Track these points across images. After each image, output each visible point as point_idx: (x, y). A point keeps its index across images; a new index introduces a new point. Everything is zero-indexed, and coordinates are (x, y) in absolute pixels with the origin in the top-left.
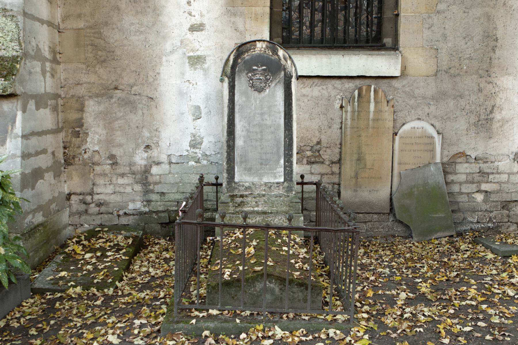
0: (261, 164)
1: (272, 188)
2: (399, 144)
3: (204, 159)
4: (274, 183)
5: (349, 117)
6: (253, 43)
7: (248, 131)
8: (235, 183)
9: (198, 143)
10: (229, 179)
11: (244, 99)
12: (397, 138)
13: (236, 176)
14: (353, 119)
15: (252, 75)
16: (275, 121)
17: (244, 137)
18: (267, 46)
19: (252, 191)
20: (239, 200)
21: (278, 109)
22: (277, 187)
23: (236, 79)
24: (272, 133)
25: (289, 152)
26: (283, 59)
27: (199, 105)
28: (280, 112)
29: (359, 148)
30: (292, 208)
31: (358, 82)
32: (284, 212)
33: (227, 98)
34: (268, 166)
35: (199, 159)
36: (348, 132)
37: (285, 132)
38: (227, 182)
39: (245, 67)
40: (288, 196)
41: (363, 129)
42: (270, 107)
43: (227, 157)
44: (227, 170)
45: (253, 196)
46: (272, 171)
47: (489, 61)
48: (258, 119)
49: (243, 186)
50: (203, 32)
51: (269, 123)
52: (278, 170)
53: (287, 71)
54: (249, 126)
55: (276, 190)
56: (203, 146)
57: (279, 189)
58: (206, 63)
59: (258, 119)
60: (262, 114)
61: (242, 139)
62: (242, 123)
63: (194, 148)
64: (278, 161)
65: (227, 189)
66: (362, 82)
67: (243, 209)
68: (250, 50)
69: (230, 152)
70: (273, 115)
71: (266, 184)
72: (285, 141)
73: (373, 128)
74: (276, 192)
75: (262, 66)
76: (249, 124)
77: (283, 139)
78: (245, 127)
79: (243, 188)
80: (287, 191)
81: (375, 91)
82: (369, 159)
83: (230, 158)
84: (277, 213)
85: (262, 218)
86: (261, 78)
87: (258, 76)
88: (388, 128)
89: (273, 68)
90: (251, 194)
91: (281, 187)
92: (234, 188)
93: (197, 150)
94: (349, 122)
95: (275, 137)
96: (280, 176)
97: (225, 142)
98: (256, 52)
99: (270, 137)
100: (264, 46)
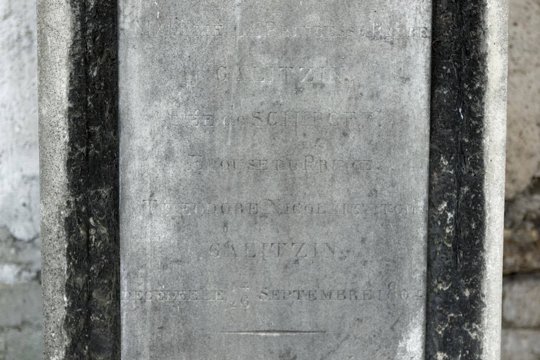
16: (374, 95)
17: (176, 192)
21: (393, 18)
24: (355, 167)
25: (456, 289)
28: (404, 41)
43: (67, 323)
48: (265, 80)
51: (332, 104)
54: (212, 128)
60: (292, 51)
61: (167, 205)
62: (163, 107)
69: (89, 287)
70: (362, 57)
72: (432, 221)
77: (421, 204)
78: (181, 131)
95: (373, 193)
97: (57, 229)
99: (339, 198)
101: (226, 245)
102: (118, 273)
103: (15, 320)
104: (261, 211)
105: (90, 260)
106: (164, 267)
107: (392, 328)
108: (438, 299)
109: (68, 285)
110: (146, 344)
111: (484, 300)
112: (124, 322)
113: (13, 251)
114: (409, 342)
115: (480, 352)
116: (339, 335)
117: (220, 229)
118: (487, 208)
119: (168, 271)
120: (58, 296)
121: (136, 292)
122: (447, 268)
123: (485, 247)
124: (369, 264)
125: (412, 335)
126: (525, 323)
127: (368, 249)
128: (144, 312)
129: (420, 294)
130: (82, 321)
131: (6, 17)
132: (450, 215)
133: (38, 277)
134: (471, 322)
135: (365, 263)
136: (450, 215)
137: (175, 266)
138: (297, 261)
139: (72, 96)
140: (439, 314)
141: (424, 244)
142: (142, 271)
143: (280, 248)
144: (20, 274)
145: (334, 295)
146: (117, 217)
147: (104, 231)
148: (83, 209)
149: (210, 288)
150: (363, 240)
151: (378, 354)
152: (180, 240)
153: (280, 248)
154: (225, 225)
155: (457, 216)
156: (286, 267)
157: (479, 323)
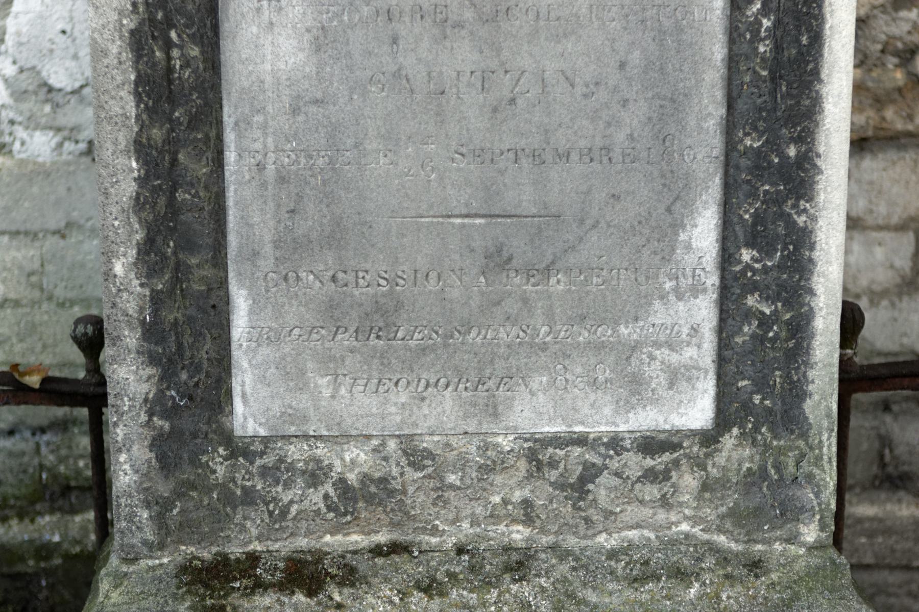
0: (497, 261)
1: (602, 490)
3: (31, 123)
4: (615, 443)
8: (239, 450)
10: (171, 412)
13: (245, 379)
22: (650, 476)
25: (773, 144)
34: (558, 284)
38: (158, 443)
40: (756, 566)
43: (139, 203)
44: (152, 332)
46: (604, 333)
49: (315, 474)
52: (660, 315)
55: (633, 512)
57: (665, 502)
65: (161, 508)
69: (172, 144)
71: (537, 454)
72: (735, 32)
74: (634, 524)
79: (316, 497)
80: (746, 520)
83: (173, 208)
90: (396, 548)
91: (689, 481)
92: (228, 498)
96: (676, 377)
101: (397, 75)
102: (219, 123)
103: (55, 221)
104: (453, 17)
105: (172, 101)
106: (295, 111)
107: (669, 210)
108: (744, 162)
109: (137, 142)
110: (268, 238)
111: (819, 162)
112: (230, 202)
113: (47, 108)
114: (696, 232)
115: (812, 248)
116: (582, 222)
117: (386, 48)
118: (827, 9)
119: (301, 118)
120: (121, 161)
122: (760, 110)
123: (823, 76)
124: (631, 105)
125: (700, 221)
126: (880, 222)
127: (630, 79)
128: (264, 185)
129: (715, 153)
130: (162, 201)
132: (766, 23)
133: (90, 150)
134: (798, 199)
135: (625, 102)
136: (766, 23)
137: (313, 109)
138: (512, 101)
140: (745, 187)
141: (723, 71)
142: (258, 119)
143: (485, 80)
144: (60, 145)
145: (574, 157)
146: (216, 28)
147: (194, 51)
148: (160, 15)
149: (371, 145)
150: (622, 65)
151: (646, 252)
152: (320, 66)
153: (485, 80)
154: (395, 41)
155: (777, 24)
156: (495, 110)
157: (810, 200)
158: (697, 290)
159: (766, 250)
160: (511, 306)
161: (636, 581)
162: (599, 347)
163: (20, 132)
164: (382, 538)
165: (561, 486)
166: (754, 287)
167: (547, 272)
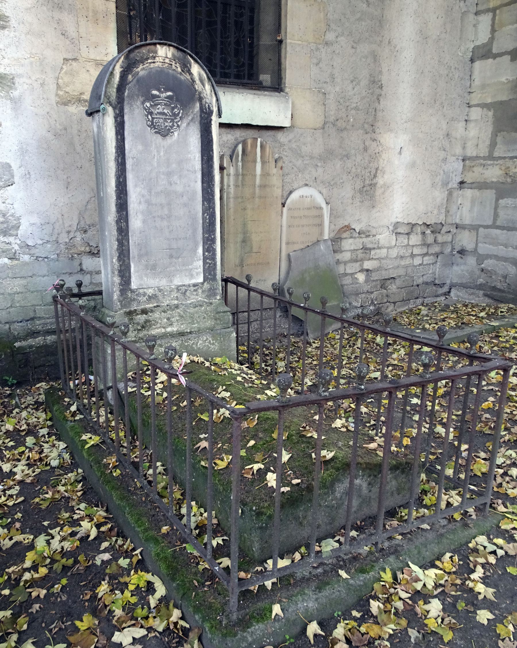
0: (171, 257)
1: (188, 293)
2: (287, 217)
3: (24, 253)
4: (189, 286)
5: (232, 183)
6: (152, 47)
7: (148, 203)
8: (132, 291)
9: (13, 227)
10: (122, 285)
11: (140, 147)
12: (285, 209)
13: (133, 279)
14: (236, 186)
15: (151, 105)
16: (189, 186)
17: (142, 213)
18: (173, 55)
19: (158, 301)
20: (141, 318)
22: (195, 290)
23: (126, 111)
24: (185, 205)
25: (210, 236)
26: (198, 82)
27: (8, 162)
28: (195, 172)
29: (245, 225)
30: (218, 322)
31: (239, 134)
32: (209, 329)
33: (114, 144)
34: (180, 260)
35: (15, 253)
36: (232, 205)
37: (203, 204)
38: (121, 291)
39: (139, 90)
40: (211, 303)
41: (249, 199)
42: (180, 162)
43: (117, 249)
44: (120, 271)
45: (161, 309)
46: (187, 267)
47: (373, 113)
49: (144, 294)
50: (6, 32)
51: (179, 188)
52: (195, 264)
53: (204, 103)
54: (150, 195)
55: (193, 297)
56: (21, 232)
57: (197, 295)
58: (16, 89)
59: (163, 182)
60: (169, 174)
61: (140, 216)
62: (138, 189)
63: (5, 236)
64: (195, 250)
66: (243, 134)
67: (150, 333)
68: (147, 59)
69: (122, 239)
71: (178, 288)
72: (204, 219)
73: (260, 197)
74: (194, 298)
75: (166, 90)
76: (150, 191)
77: (201, 214)
78: (143, 196)
79: (145, 299)
80: (209, 297)
81: (262, 146)
82: (255, 239)
84: (200, 332)
85: (180, 342)
86: (166, 111)
87: (160, 108)
88: (277, 197)
89: (184, 96)
90: (158, 306)
91: (200, 291)
92: (131, 299)
93: (11, 239)
94: (232, 190)
95: (190, 212)
96: (198, 274)
98: (156, 65)
100: (170, 55)
103: (30, 274)
121: (133, 240)
131: (20, 167)
139: (116, 187)
158: (200, 260)
159: (209, 252)
160: (173, 264)
161: (195, 307)
162: (186, 270)
163: (21, 255)
164: (155, 305)
165: (182, 293)
166: (208, 259)
167: (178, 258)
